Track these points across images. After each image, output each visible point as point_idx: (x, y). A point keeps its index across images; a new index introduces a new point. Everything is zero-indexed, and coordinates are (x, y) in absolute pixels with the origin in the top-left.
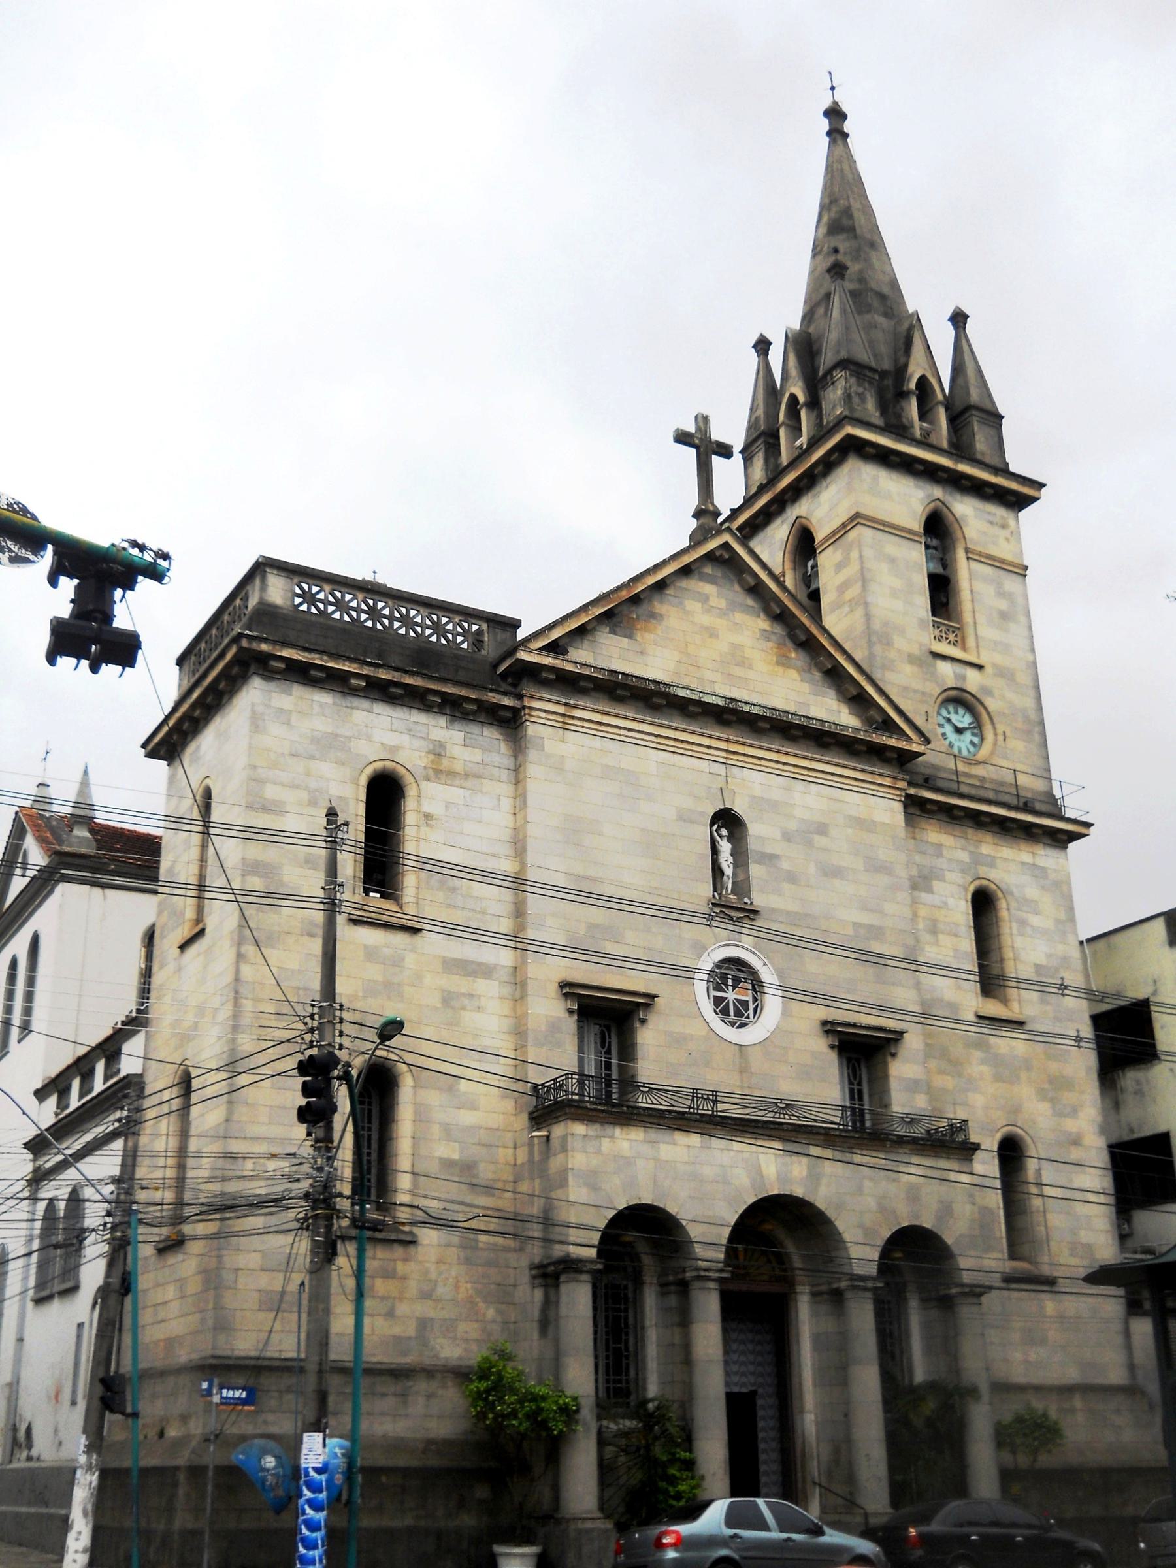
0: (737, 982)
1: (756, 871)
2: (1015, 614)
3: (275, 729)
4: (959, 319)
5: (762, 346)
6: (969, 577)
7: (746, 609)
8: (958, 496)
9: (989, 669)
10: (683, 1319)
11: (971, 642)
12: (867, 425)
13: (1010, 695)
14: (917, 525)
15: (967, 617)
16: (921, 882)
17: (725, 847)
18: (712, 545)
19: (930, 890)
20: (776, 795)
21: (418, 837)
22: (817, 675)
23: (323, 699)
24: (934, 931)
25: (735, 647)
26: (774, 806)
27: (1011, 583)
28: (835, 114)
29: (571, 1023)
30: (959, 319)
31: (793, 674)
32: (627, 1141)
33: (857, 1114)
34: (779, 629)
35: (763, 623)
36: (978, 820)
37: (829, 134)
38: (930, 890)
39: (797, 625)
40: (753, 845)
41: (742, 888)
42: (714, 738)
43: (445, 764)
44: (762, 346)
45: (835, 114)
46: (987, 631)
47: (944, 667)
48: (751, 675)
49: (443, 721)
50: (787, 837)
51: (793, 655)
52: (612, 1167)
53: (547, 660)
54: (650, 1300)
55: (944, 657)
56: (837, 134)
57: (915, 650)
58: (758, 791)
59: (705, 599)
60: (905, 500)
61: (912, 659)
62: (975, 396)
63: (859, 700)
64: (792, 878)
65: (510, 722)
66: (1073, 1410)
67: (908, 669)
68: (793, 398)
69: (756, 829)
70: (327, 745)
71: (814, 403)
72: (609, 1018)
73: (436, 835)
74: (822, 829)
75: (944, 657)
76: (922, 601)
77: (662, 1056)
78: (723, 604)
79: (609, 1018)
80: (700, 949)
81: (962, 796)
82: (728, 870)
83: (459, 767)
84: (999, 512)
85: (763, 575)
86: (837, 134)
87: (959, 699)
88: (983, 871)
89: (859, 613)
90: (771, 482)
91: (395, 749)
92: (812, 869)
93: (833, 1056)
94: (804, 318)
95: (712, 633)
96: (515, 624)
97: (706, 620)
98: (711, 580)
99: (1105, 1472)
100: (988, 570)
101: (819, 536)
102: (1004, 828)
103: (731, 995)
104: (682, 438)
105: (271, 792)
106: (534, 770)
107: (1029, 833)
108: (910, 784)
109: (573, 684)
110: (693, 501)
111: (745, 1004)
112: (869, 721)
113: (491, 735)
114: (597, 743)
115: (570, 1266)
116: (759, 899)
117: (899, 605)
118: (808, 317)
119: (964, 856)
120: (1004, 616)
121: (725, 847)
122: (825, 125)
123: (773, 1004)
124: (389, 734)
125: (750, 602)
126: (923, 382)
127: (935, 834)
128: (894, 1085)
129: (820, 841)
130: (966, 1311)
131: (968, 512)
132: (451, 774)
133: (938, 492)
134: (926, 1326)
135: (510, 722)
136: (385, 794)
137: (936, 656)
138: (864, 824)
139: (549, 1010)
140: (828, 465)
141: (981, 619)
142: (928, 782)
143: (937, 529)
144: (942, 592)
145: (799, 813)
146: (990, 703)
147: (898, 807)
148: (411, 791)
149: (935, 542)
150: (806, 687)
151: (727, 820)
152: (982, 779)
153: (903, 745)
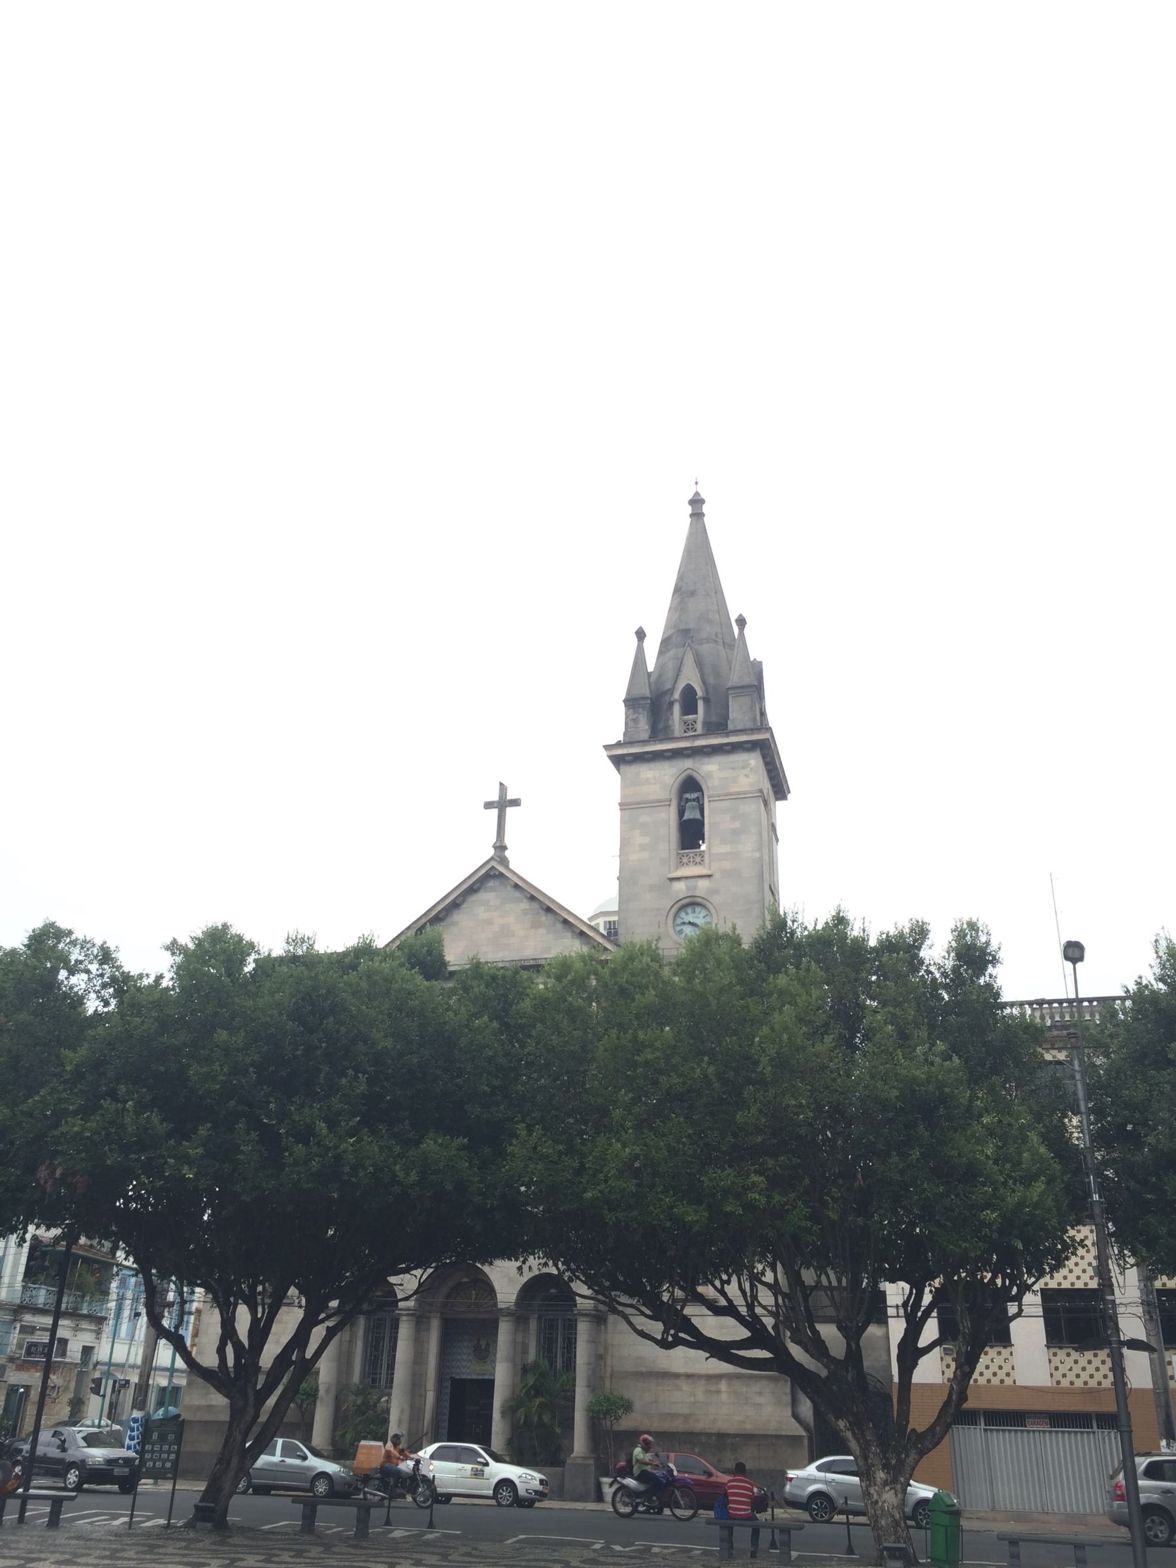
4: (741, 622)
8: (706, 760)
9: (717, 876)
28: (697, 502)
31: (542, 931)
35: (525, 905)
37: (691, 516)
45: (697, 502)
47: (680, 886)
51: (544, 919)
55: (678, 879)
56: (697, 515)
66: (719, 1392)
75: (678, 879)
86: (697, 515)
98: (492, 889)
99: (722, 1436)
100: (726, 804)
125: (517, 894)
133: (688, 763)
137: (672, 879)
143: (690, 786)
146: (716, 899)
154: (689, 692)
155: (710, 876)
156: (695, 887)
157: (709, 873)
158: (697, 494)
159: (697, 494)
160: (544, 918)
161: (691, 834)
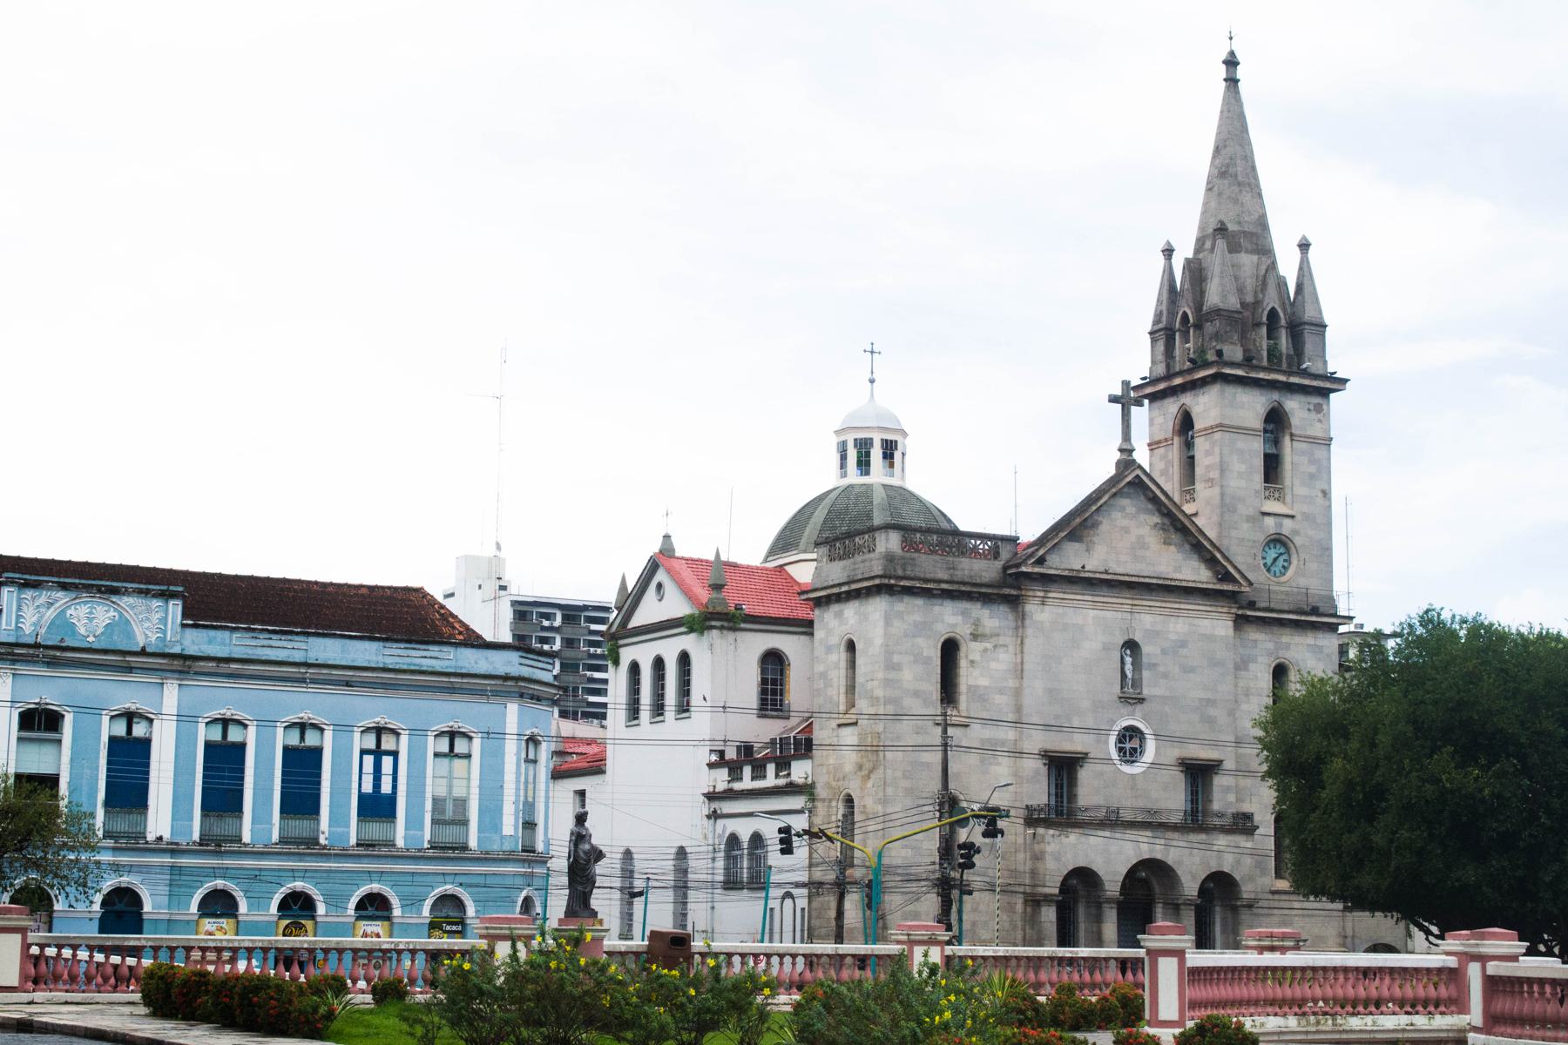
0: (1131, 738)
1: (1146, 674)
2: (1321, 474)
3: (896, 623)
4: (1304, 246)
5: (1168, 252)
6: (1290, 453)
7: (1147, 511)
9: (1299, 517)
10: (1098, 919)
11: (1288, 498)
12: (1232, 364)
13: (1311, 532)
14: (1258, 424)
15: (1288, 482)
16: (1241, 666)
17: (1128, 660)
18: (1129, 478)
19: (1246, 669)
20: (1159, 627)
21: (969, 677)
22: (1187, 547)
23: (919, 602)
24: (1247, 695)
25: (1140, 537)
26: (1157, 633)
27: (1319, 453)
28: (1231, 62)
29: (1044, 770)
30: (1304, 246)
31: (1173, 548)
32: (1073, 838)
33: (1194, 812)
34: (1166, 521)
35: (1157, 519)
36: (1281, 623)
38: (1246, 669)
39: (1178, 527)
40: (1145, 660)
41: (1137, 683)
42: (1125, 601)
43: (980, 630)
44: (1168, 252)
45: (1231, 62)
46: (1301, 490)
47: (1269, 521)
48: (1148, 554)
49: (979, 605)
50: (1164, 652)
52: (1068, 850)
53: (1036, 570)
54: (1081, 911)
55: (1269, 514)
56: (1232, 81)
57: (1251, 511)
58: (1148, 626)
59: (1123, 509)
60: (1251, 407)
61: (1250, 519)
62: (1309, 314)
63: (1211, 561)
64: (1165, 676)
65: (1014, 602)
67: (1246, 526)
68: (1185, 315)
69: (1147, 649)
70: (922, 628)
71: (1198, 326)
72: (1063, 767)
73: (976, 672)
74: (1183, 644)
75: (1269, 514)
76: (1259, 477)
77: (1090, 790)
78: (1134, 510)
79: (1063, 767)
80: (1113, 722)
81: (1272, 611)
82: (1129, 675)
83: (987, 631)
84: (1316, 400)
85: (1158, 492)
86: (1232, 81)
87: (1278, 541)
88: (1282, 653)
89: (1217, 490)
90: (1169, 376)
91: (955, 625)
92: (1177, 669)
93: (1182, 776)
94: (1198, 240)
95: (1126, 530)
96: (1013, 540)
97: (1125, 522)
98: (1128, 496)
101: (1197, 427)
102: (1298, 626)
103: (1128, 746)
104: (1114, 399)
105: (896, 658)
106: (1029, 631)
107: (1314, 626)
108: (1240, 608)
109: (1048, 580)
110: (1117, 441)
111: (1135, 749)
112: (1216, 573)
113: (1003, 609)
114: (1060, 610)
115: (1047, 899)
116: (1146, 692)
117: (1243, 483)
118: (1198, 250)
119: (1271, 646)
120: (1312, 477)
121: (1128, 660)
122: (1222, 71)
123: (1151, 745)
124: (950, 618)
126: (1273, 314)
127: (1255, 635)
128: (1215, 789)
129: (1183, 651)
130: (1245, 916)
131: (1294, 406)
132: (983, 635)
133: (1276, 396)
134: (1224, 919)
135: (1014, 602)
136: (950, 650)
138: (1211, 638)
139: (1035, 767)
140: (1204, 382)
141: (1296, 482)
142: (1252, 605)
144: (1272, 467)
145: (1172, 637)
146: (1298, 540)
147: (1231, 624)
148: (963, 649)
149: (1271, 427)
150: (1180, 556)
151: (1131, 646)
152: (1287, 594)
153: (1236, 588)
154: (1273, 314)
155: (1292, 517)
156: (1281, 525)
157: (1290, 512)
158: (1232, 53)
159: (1232, 53)
160: (1175, 537)
161: (1272, 467)
